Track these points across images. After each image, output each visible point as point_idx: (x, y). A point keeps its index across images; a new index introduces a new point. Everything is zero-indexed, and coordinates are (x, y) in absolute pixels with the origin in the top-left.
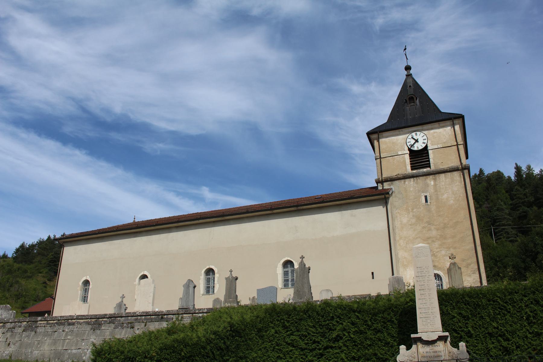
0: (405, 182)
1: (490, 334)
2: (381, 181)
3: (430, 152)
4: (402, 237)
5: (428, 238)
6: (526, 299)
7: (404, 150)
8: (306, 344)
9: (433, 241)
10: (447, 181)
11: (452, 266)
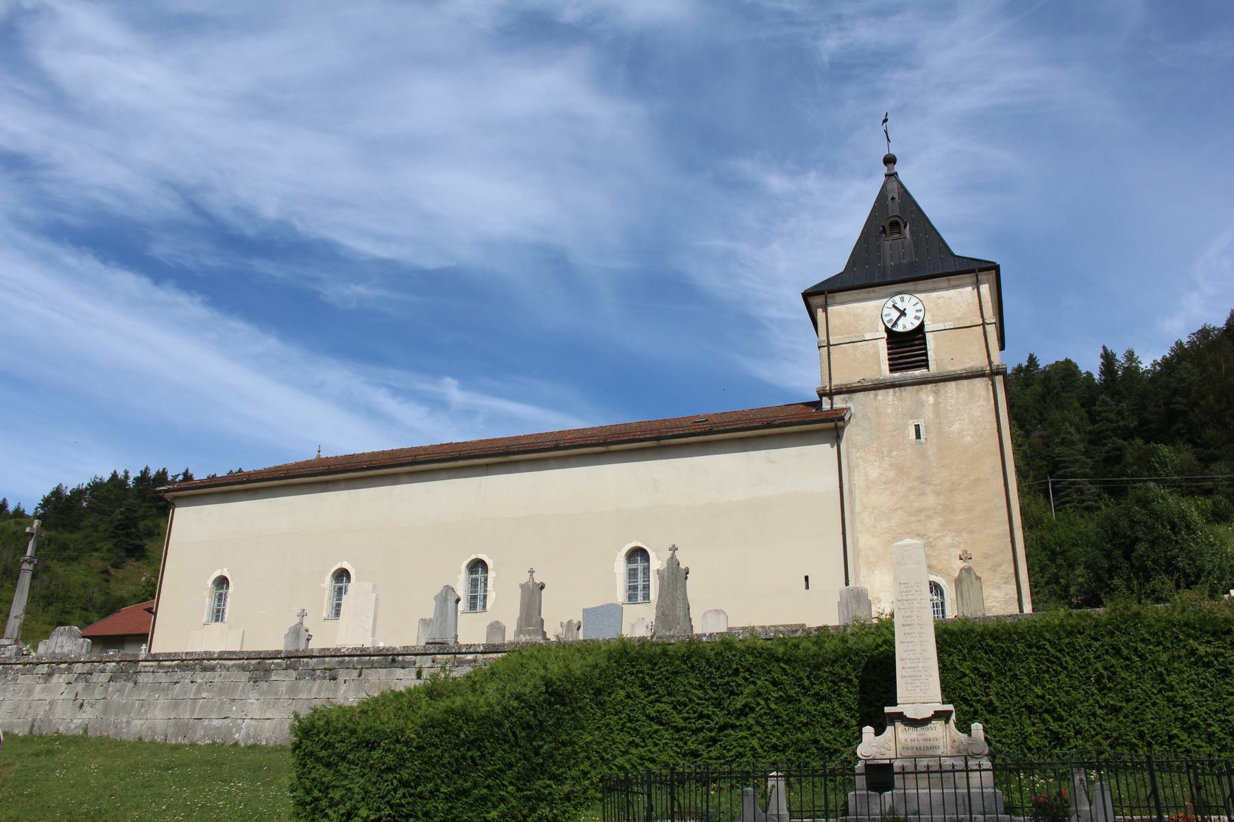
0: (876, 395)
1: (1030, 709)
2: (828, 391)
3: (929, 337)
4: (867, 508)
5: (920, 511)
6: (1097, 644)
7: (877, 331)
8: (685, 719)
9: (929, 517)
11: (964, 574)
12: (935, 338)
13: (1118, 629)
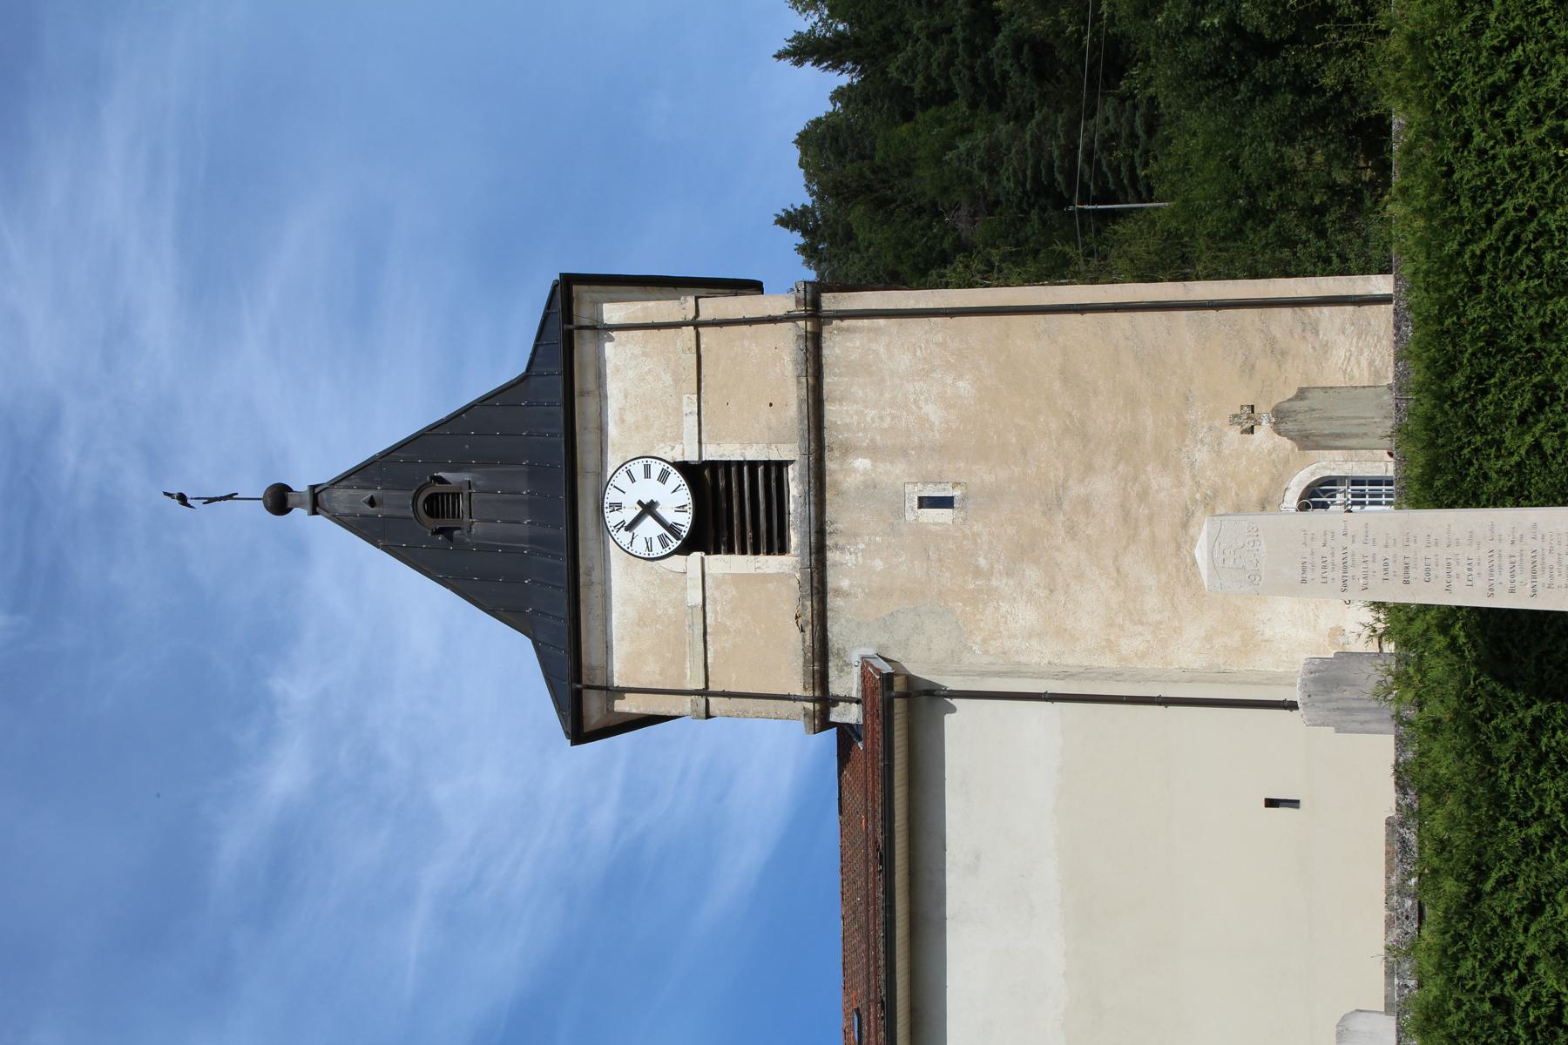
0: (838, 592)
2: (817, 707)
3: (712, 453)
4: (1108, 641)
5: (1126, 515)
6: (1479, 137)
7: (685, 573)
9: (1143, 495)
10: (860, 393)
11: (1290, 426)
12: (718, 440)
13: (1445, 86)
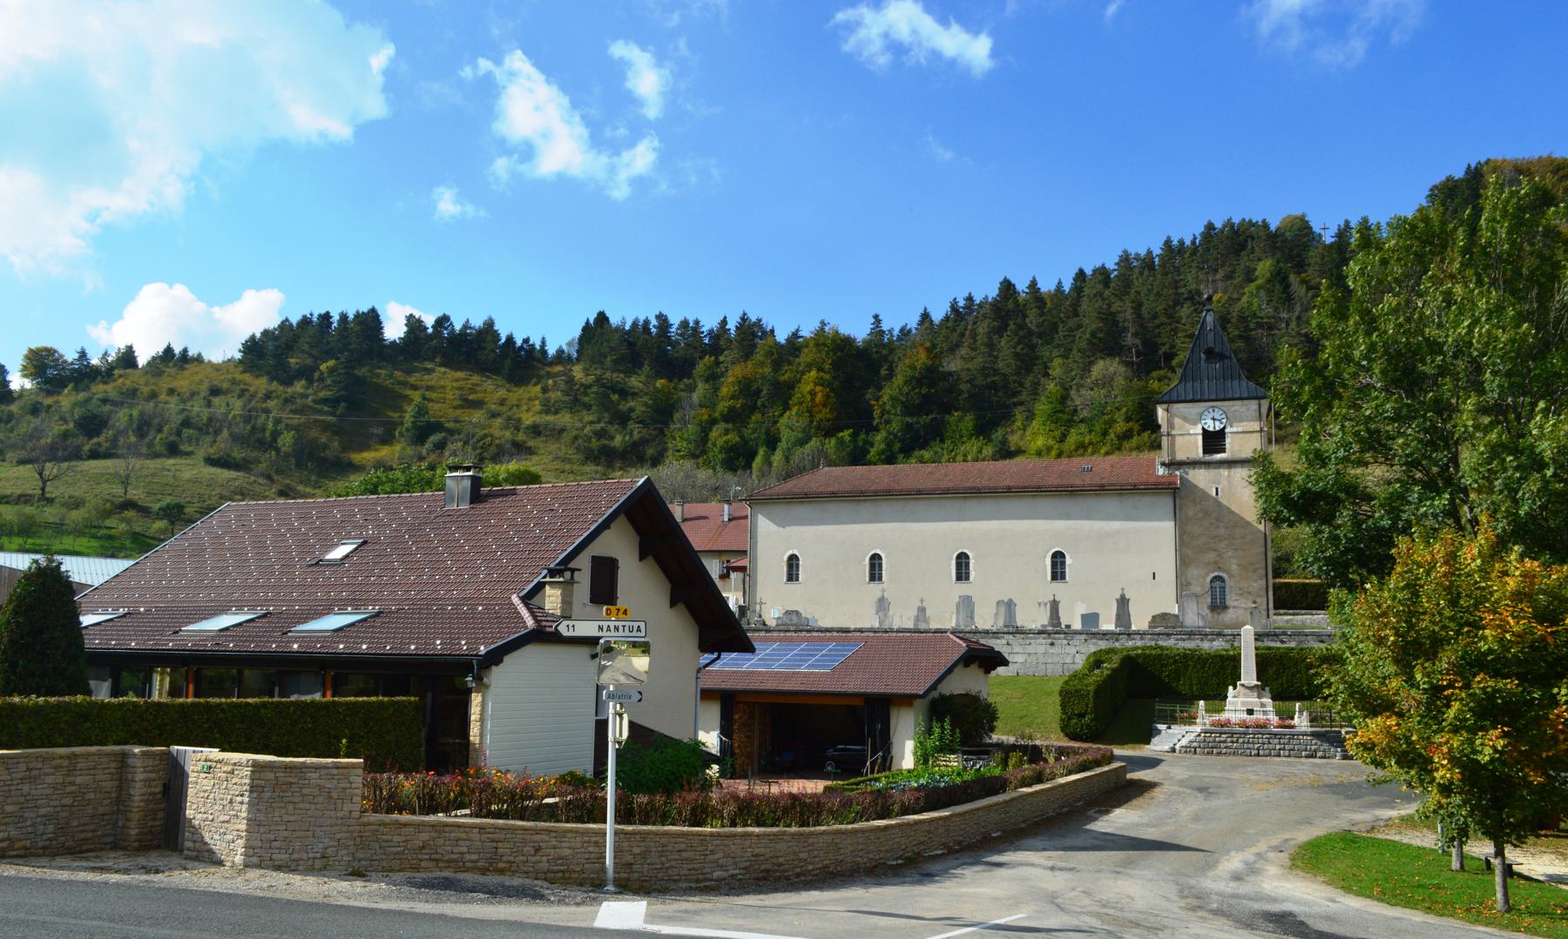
5: (1216, 536)
9: (1220, 541)
